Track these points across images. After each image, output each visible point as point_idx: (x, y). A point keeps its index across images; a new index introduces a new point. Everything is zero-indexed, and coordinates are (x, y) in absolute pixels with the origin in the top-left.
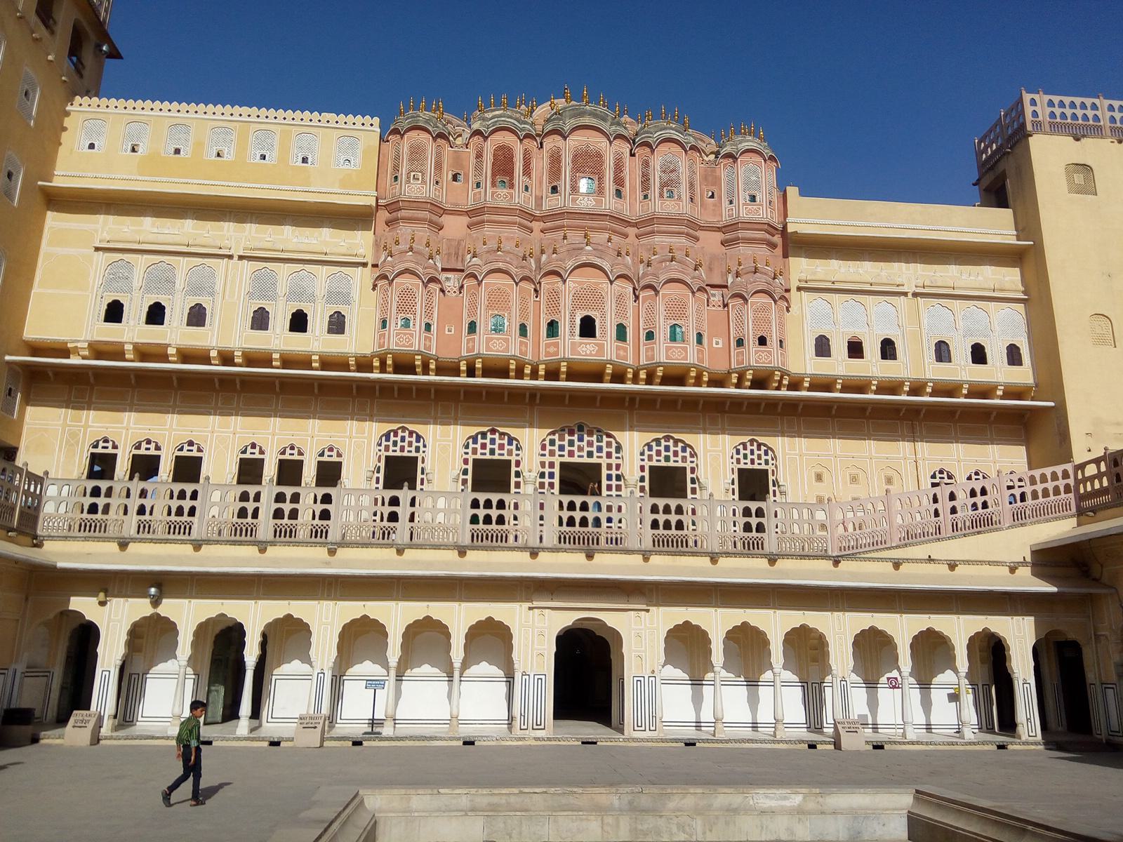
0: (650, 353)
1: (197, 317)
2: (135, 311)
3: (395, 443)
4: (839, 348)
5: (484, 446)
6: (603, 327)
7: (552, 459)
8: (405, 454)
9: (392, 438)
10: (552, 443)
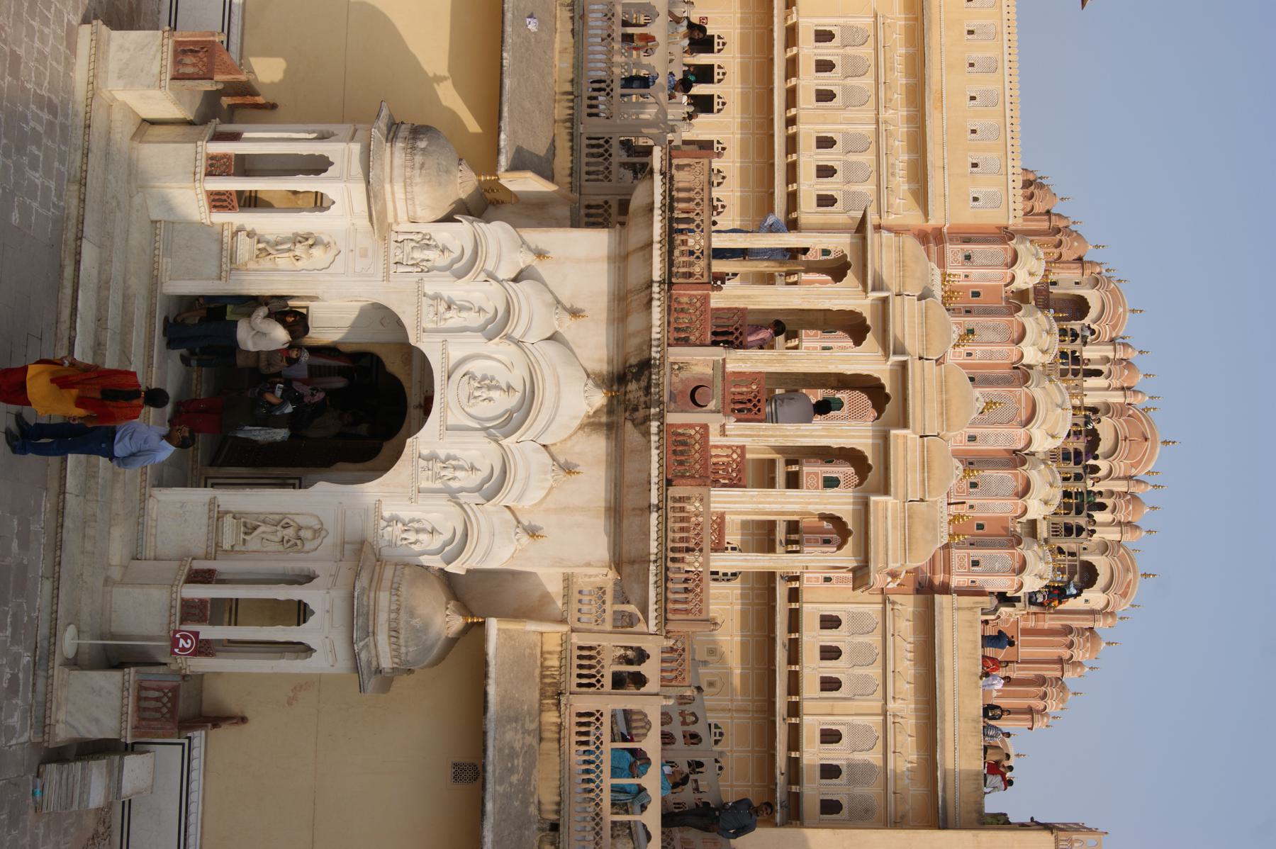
1: (825, 96)
2: (826, 51)
4: (830, 638)
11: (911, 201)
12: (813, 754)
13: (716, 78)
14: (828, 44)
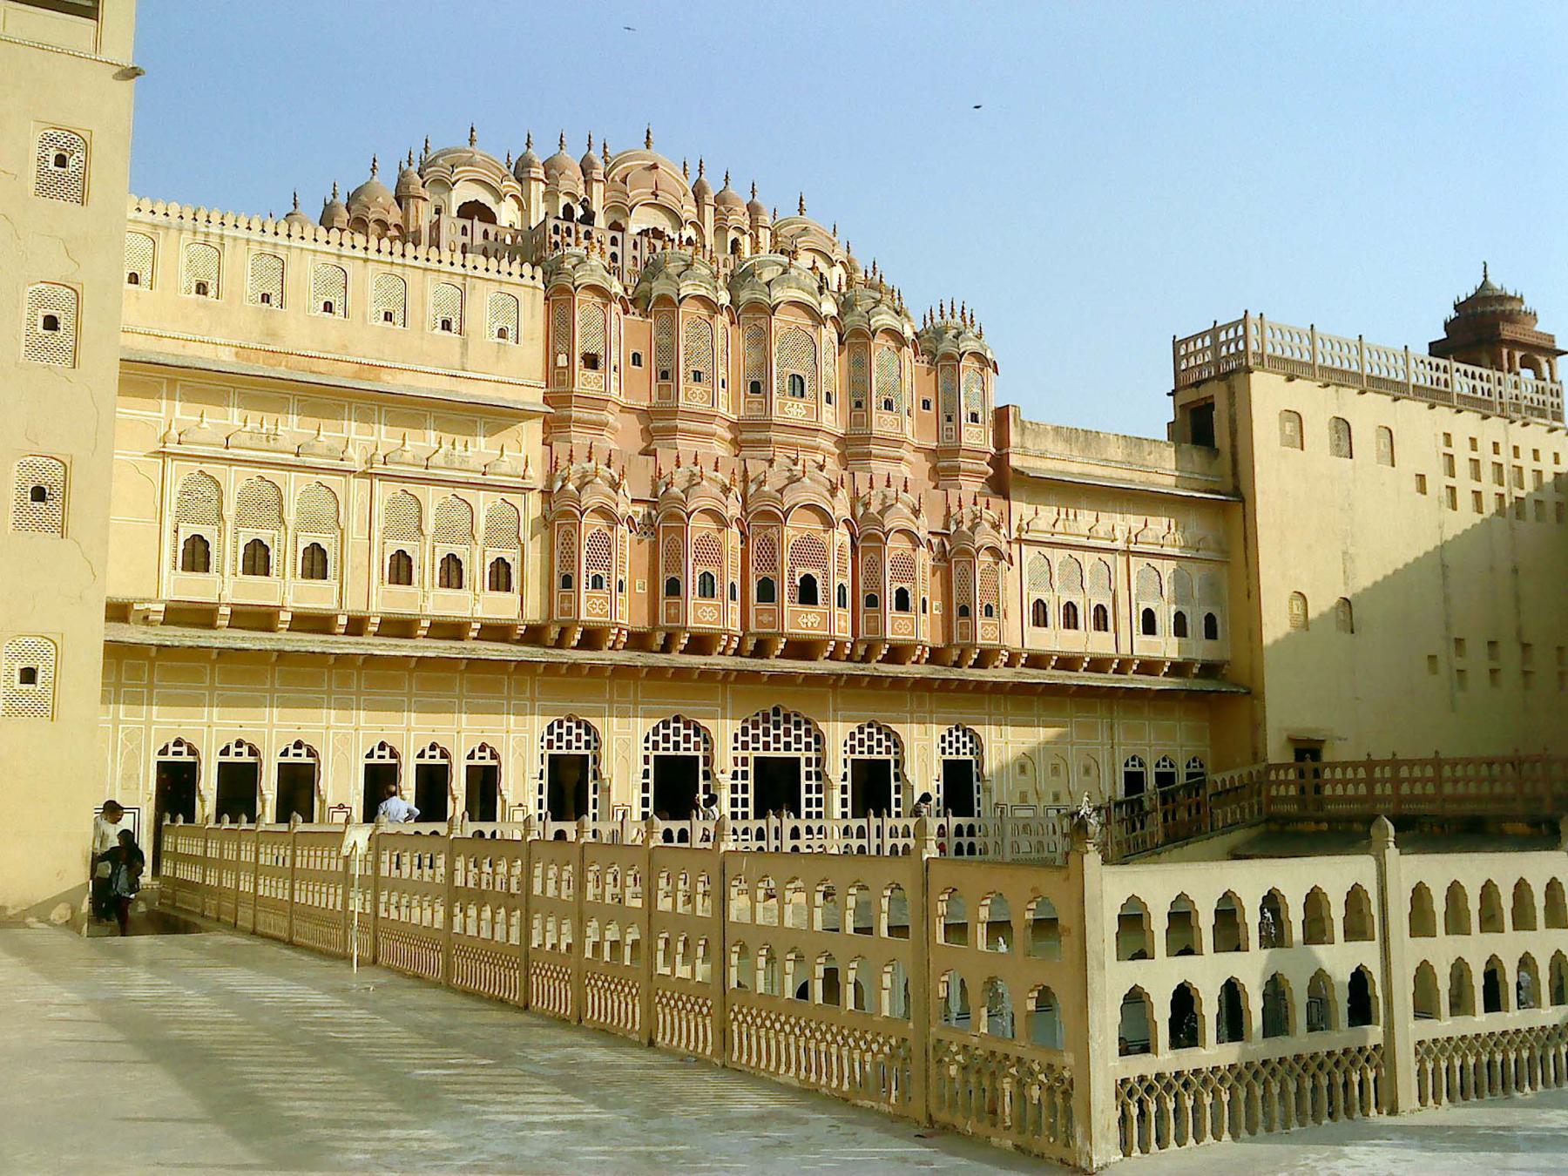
0: (872, 624)
2: (228, 550)
3: (560, 738)
5: (666, 738)
6: (826, 590)
7: (745, 754)
8: (573, 751)
9: (556, 730)
10: (745, 732)
11: (505, 437)
12: (1165, 646)
13: (246, 758)
14: (213, 549)
